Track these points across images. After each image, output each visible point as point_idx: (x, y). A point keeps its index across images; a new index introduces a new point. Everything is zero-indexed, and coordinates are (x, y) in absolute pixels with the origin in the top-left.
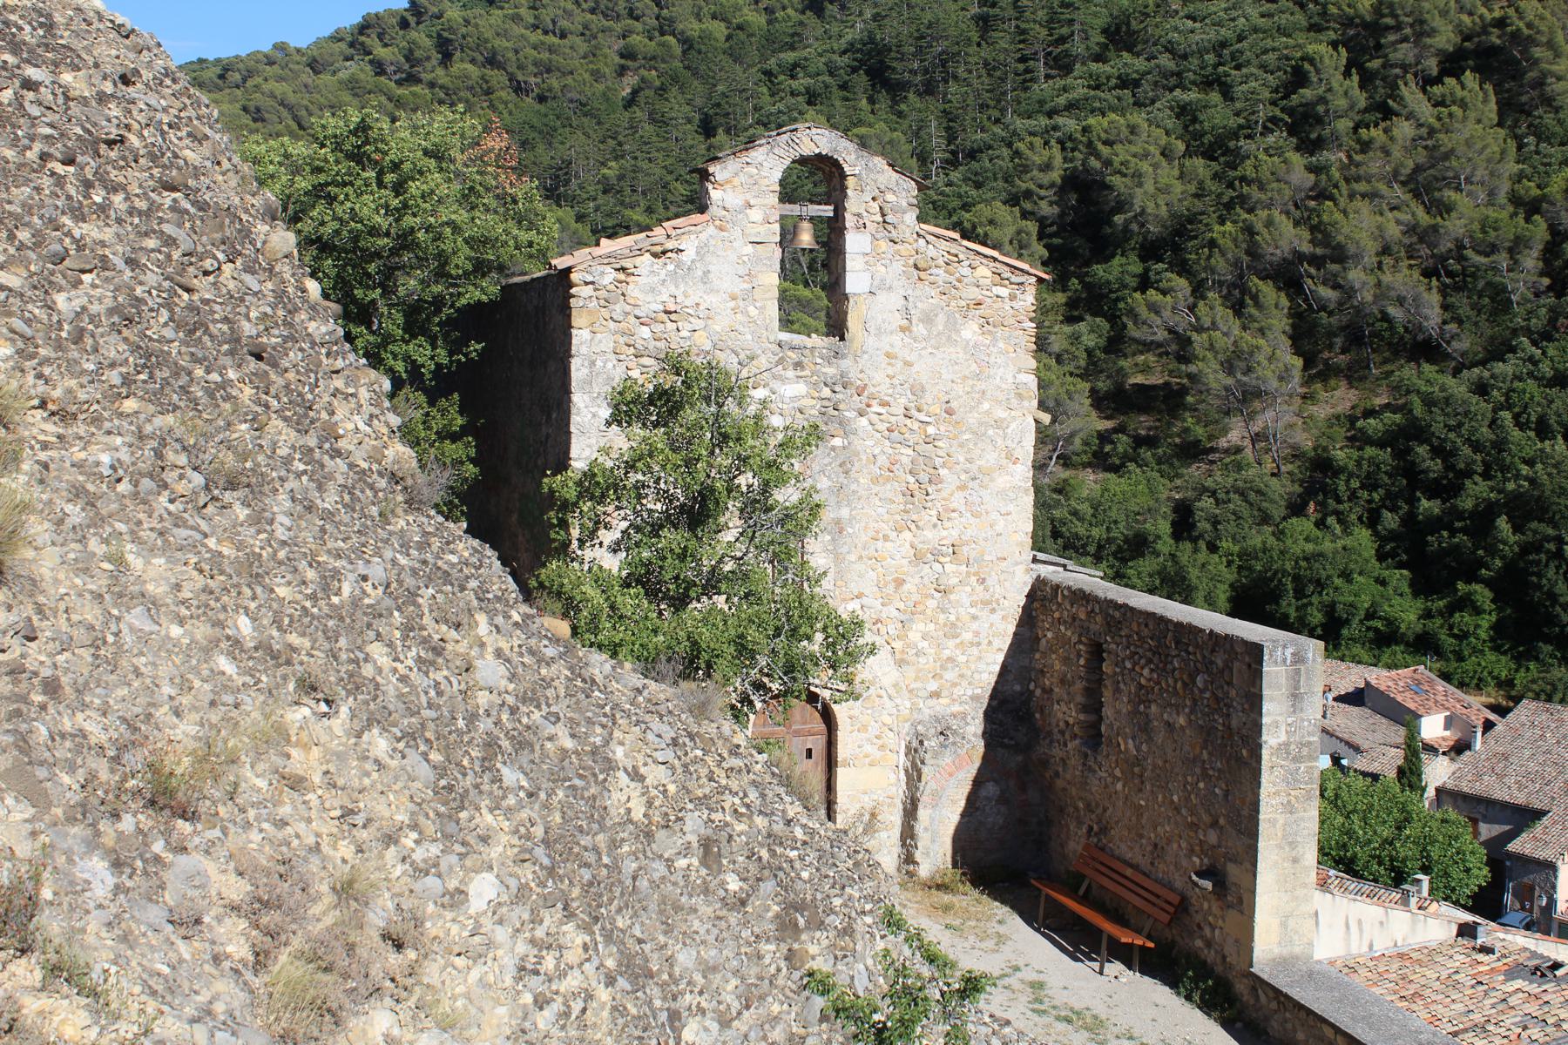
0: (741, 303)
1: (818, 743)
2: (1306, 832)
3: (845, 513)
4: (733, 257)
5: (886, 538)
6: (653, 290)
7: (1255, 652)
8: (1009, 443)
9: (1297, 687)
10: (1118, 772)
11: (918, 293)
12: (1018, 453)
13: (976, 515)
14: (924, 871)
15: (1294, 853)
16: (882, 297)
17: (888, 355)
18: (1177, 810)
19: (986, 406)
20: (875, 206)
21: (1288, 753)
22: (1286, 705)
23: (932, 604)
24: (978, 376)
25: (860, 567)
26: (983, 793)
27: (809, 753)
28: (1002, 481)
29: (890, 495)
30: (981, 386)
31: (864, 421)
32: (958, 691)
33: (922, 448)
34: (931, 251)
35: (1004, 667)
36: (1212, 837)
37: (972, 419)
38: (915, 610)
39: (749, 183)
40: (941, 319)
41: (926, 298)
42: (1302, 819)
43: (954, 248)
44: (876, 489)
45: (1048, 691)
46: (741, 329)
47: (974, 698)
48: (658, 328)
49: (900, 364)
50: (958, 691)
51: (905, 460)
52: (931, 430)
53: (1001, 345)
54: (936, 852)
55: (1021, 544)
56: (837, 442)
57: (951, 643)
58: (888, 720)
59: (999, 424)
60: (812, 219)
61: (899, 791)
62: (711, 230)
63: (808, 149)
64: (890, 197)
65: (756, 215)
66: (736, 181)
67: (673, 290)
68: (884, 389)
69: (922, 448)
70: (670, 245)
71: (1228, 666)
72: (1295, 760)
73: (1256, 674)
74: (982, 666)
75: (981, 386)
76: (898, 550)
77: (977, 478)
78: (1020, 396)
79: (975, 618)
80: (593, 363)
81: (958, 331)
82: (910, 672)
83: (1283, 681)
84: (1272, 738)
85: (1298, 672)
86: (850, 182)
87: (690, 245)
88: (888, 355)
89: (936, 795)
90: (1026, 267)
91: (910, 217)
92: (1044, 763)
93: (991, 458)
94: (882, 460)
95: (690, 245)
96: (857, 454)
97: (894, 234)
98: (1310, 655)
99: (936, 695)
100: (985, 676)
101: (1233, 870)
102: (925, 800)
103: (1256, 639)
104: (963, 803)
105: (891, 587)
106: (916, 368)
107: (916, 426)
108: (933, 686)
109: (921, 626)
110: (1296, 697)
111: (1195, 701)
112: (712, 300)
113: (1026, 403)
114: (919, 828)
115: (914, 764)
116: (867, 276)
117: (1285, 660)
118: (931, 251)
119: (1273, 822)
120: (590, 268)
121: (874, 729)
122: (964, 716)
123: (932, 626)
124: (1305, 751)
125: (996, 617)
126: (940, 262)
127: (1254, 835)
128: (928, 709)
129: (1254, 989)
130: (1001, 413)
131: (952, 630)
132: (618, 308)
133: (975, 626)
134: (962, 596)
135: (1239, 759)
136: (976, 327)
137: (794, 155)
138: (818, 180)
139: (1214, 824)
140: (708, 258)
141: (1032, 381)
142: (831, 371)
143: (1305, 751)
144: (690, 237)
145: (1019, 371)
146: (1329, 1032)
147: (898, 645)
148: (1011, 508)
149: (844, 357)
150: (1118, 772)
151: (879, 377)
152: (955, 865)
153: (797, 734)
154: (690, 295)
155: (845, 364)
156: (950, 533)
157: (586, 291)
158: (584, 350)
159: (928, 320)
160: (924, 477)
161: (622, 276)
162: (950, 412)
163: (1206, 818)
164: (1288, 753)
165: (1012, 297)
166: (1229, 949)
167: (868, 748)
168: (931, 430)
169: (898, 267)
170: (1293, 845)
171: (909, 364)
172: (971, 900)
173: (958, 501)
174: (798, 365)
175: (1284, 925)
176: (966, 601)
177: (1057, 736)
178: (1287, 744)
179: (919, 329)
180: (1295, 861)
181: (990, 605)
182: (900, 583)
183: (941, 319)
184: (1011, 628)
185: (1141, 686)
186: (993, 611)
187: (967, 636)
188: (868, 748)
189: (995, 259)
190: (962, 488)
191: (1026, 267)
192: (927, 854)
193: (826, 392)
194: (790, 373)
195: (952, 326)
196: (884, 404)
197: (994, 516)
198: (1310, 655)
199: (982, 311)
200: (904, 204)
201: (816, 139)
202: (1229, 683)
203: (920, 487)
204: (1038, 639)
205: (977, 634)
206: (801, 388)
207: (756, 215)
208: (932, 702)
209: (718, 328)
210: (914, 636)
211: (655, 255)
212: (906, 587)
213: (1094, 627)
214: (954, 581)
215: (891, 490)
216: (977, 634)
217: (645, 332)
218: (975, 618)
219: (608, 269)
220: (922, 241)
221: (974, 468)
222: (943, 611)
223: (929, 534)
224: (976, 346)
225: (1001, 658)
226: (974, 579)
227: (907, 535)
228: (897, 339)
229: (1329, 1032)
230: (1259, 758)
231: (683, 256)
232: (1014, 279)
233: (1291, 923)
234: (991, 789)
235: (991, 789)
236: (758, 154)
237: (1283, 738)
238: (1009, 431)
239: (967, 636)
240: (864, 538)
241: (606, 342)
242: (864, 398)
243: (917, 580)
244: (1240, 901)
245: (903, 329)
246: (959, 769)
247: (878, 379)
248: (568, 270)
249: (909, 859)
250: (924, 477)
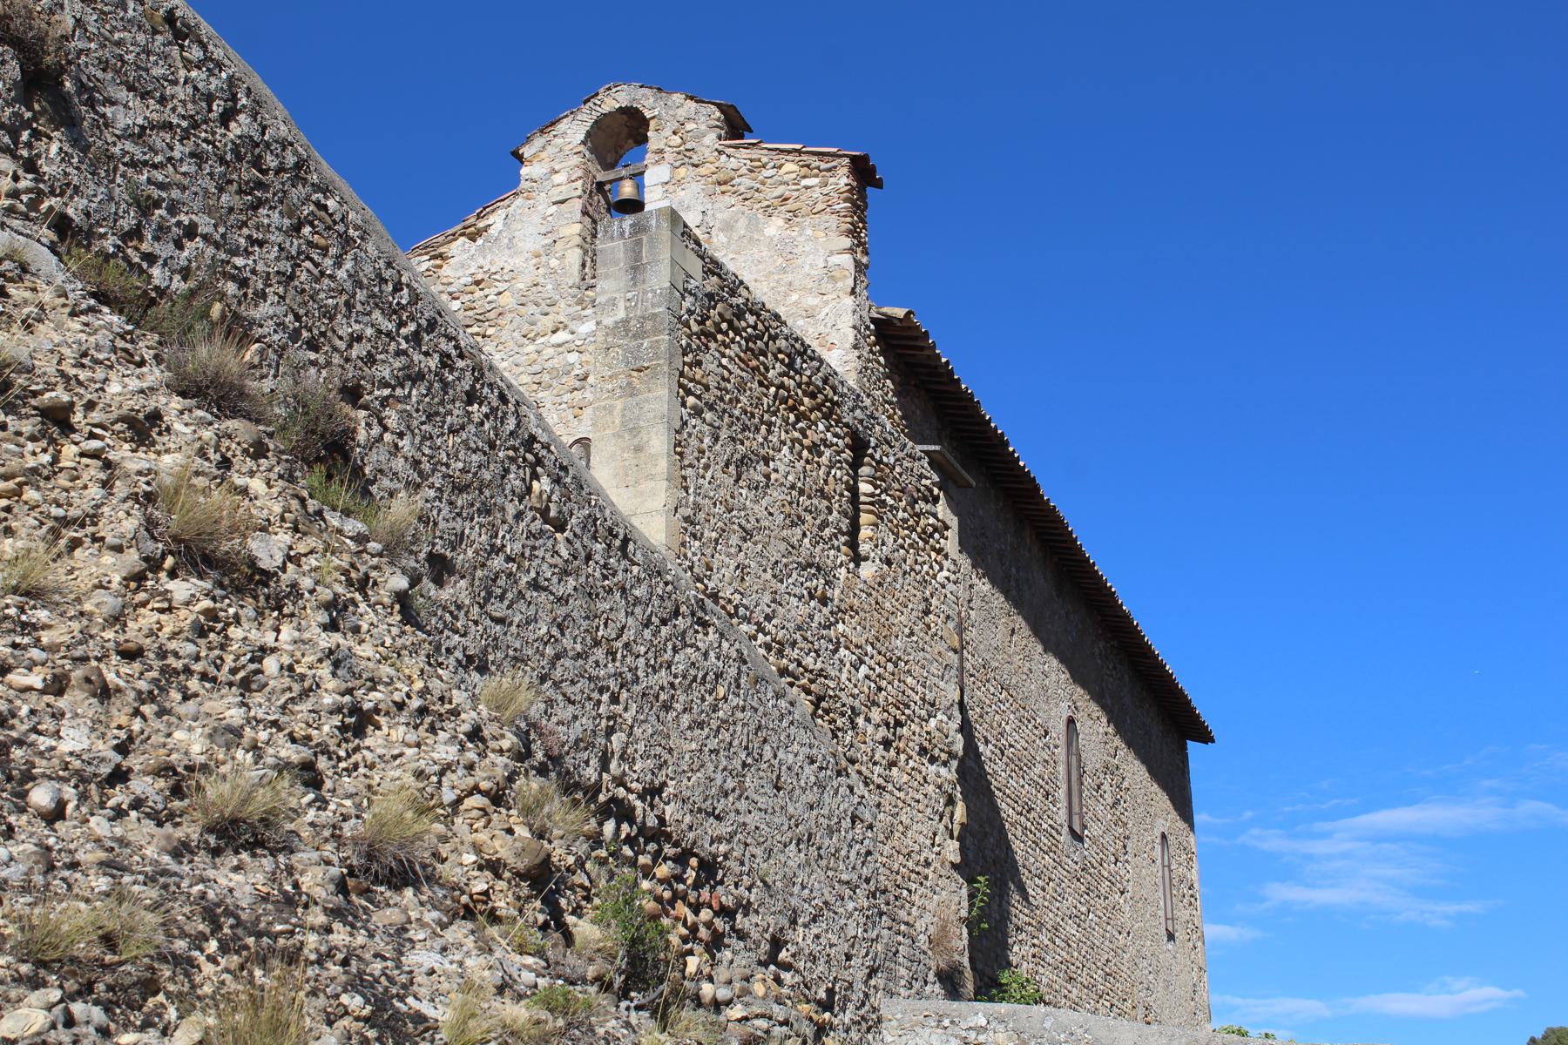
0: (544, 259)
2: (651, 415)
4: (536, 219)
8: (821, 329)
11: (717, 206)
15: (636, 442)
20: (676, 140)
21: (627, 331)
22: (624, 279)
30: (790, 277)
34: (733, 163)
42: (647, 400)
43: (755, 153)
46: (541, 280)
53: (809, 232)
62: (519, 201)
64: (690, 126)
65: (560, 178)
66: (543, 155)
67: (481, 261)
70: (481, 224)
72: (635, 337)
75: (790, 277)
78: (833, 279)
81: (760, 231)
85: (639, 243)
87: (496, 220)
91: (711, 139)
97: (695, 160)
98: (653, 222)
110: (636, 268)
112: (517, 262)
113: (840, 285)
117: (622, 234)
118: (733, 163)
124: (649, 325)
126: (744, 170)
130: (812, 301)
136: (781, 222)
137: (595, 115)
140: (515, 226)
141: (847, 260)
145: (831, 253)
161: (438, 262)
164: (627, 331)
169: (695, 187)
170: (634, 431)
178: (626, 321)
183: (743, 222)
189: (799, 152)
195: (753, 225)
198: (653, 222)
199: (791, 205)
200: (703, 127)
209: (521, 286)
211: (473, 238)
220: (723, 157)
224: (782, 240)
231: (491, 231)
232: (823, 166)
237: (621, 314)
238: (821, 316)
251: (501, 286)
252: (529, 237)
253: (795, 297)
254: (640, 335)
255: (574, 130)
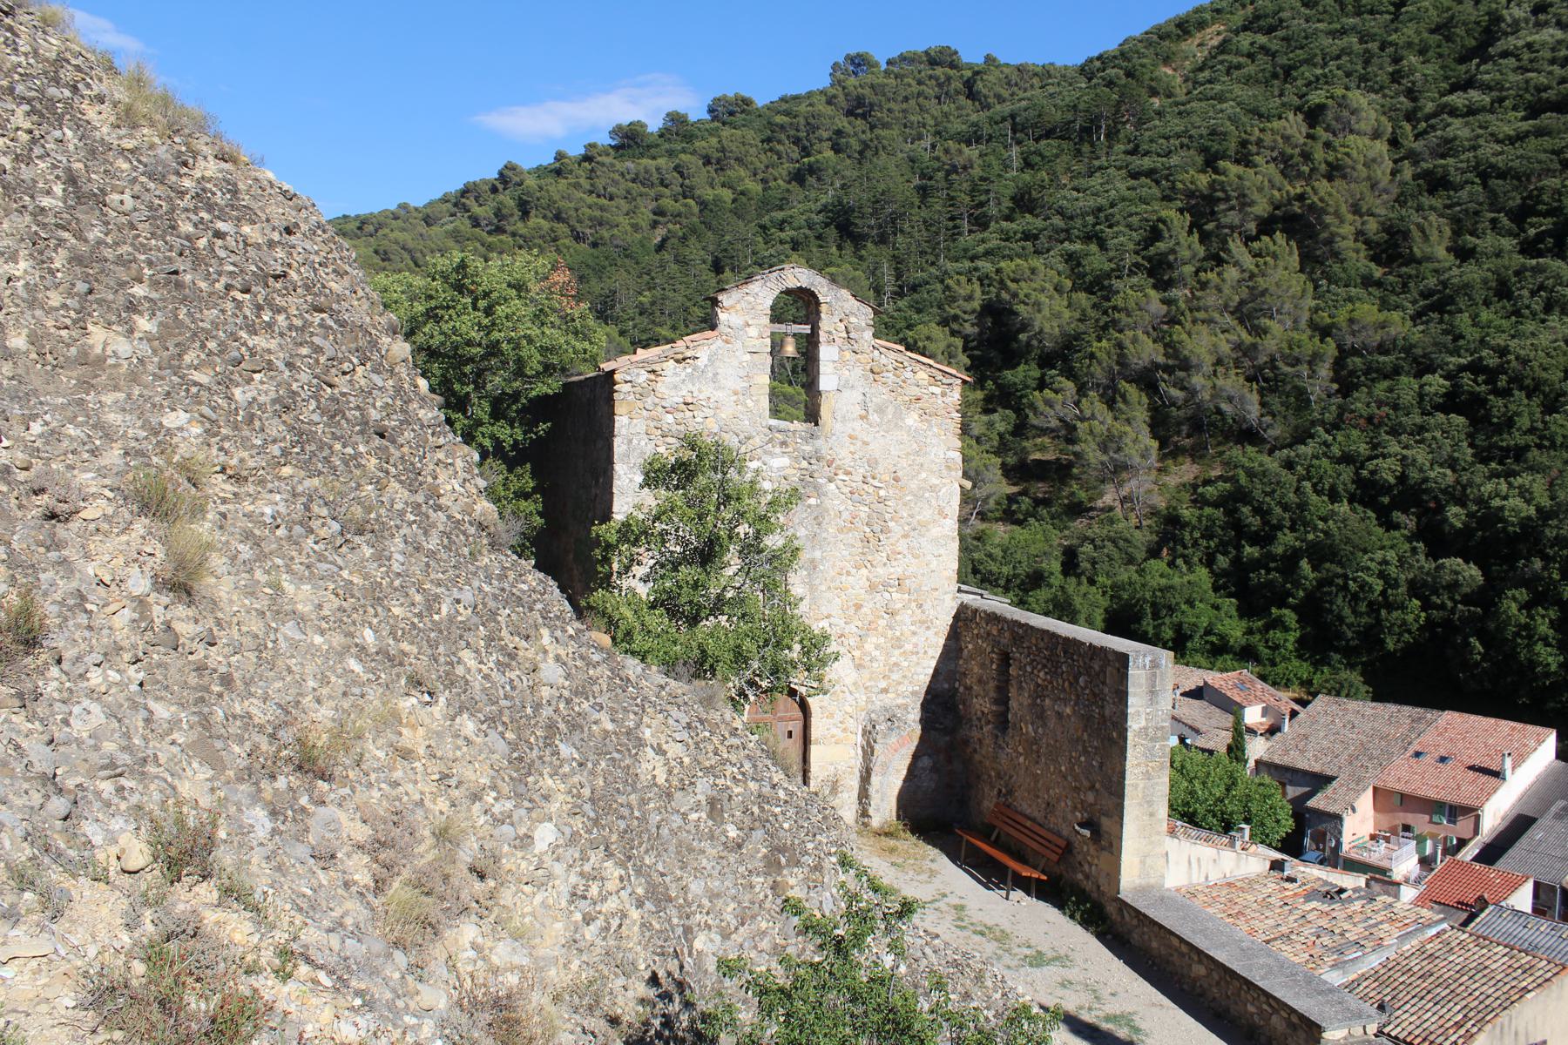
1: (796, 727)
3: (818, 554)
5: (848, 573)
6: (675, 387)
7: (1123, 659)
9: (1153, 686)
10: (1020, 749)
12: (948, 510)
13: (916, 557)
14: (876, 822)
16: (846, 393)
17: (851, 437)
18: (1065, 777)
19: (924, 475)
20: (842, 326)
23: (882, 623)
24: (917, 453)
25: (828, 595)
26: (920, 764)
27: (790, 734)
28: (935, 531)
29: (852, 541)
30: (920, 460)
31: (832, 486)
32: (902, 688)
33: (876, 506)
34: (883, 360)
35: (936, 670)
36: (1090, 797)
37: (914, 485)
38: (870, 627)
39: (747, 309)
40: (891, 410)
41: (880, 395)
43: (900, 358)
44: (841, 537)
45: (968, 688)
47: (914, 693)
48: (679, 415)
49: (859, 443)
50: (902, 688)
51: (863, 515)
52: (882, 493)
54: (885, 807)
55: (949, 578)
56: (812, 501)
57: (897, 652)
58: (849, 710)
59: (933, 488)
60: (794, 335)
61: (857, 762)
62: (719, 343)
63: (792, 283)
64: (853, 319)
65: (753, 332)
66: (738, 307)
68: (847, 462)
69: (876, 506)
70: (688, 354)
71: (1103, 670)
73: (1123, 676)
74: (920, 670)
75: (920, 460)
76: (857, 582)
77: (917, 528)
78: (948, 468)
79: (914, 633)
80: (630, 441)
82: (866, 674)
83: (1143, 681)
84: (1135, 724)
85: (1154, 675)
86: (823, 308)
88: (851, 437)
89: (885, 766)
90: (953, 372)
91: (868, 334)
92: (966, 742)
93: (927, 514)
94: (846, 515)
95: (703, 355)
96: (827, 511)
97: (856, 347)
99: (885, 691)
100: (922, 677)
101: (1105, 822)
102: (876, 769)
103: (1123, 650)
104: (905, 772)
105: (852, 611)
106: (871, 447)
107: (871, 490)
108: (883, 684)
109: (874, 640)
110: (1153, 693)
111: (1078, 696)
112: (720, 395)
114: (872, 791)
115: (868, 743)
116: (835, 378)
118: (883, 360)
119: (1136, 786)
120: (630, 371)
121: (838, 716)
122: (905, 707)
123: (882, 640)
124: (1159, 734)
125: (930, 633)
126: (890, 367)
127: (1121, 796)
128: (879, 701)
129: (1120, 910)
130: (935, 481)
131: (897, 643)
132: (650, 400)
133: (914, 639)
134: (905, 617)
135: (1111, 739)
136: (916, 417)
138: (800, 306)
139: (1092, 787)
140: (717, 363)
141: (958, 457)
142: (808, 448)
143: (1159, 734)
144: (703, 347)
146: (1175, 942)
147: (857, 653)
148: (942, 551)
149: (818, 438)
150: (1020, 749)
151: (844, 453)
152: (898, 818)
153: (781, 719)
154: (703, 391)
155: (819, 443)
156: (896, 570)
157: (626, 388)
158: (624, 431)
159: (880, 410)
160: (877, 528)
161: (652, 377)
162: (896, 480)
163: (1086, 783)
165: (944, 395)
166: (1102, 881)
167: (834, 731)
168: (882, 493)
169: (858, 371)
170: (1150, 803)
171: (866, 443)
172: (911, 845)
173: (902, 546)
174: (784, 444)
175: (1143, 862)
176: (908, 621)
177: (975, 722)
178: (1146, 728)
179: (874, 417)
180: (1152, 815)
181: (926, 624)
182: (858, 607)
183: (891, 410)
184: (942, 641)
185: (1038, 685)
186: (928, 628)
187: (908, 647)
188: (834, 731)
190: (905, 536)
191: (953, 372)
192: (878, 810)
193: (804, 464)
194: (778, 450)
195: (898, 415)
196: (848, 473)
197: (929, 557)
201: (798, 276)
202: (1104, 683)
203: (874, 536)
204: (961, 650)
205: (916, 645)
206: (786, 461)
207: (753, 332)
208: (882, 696)
210: (869, 647)
211: (677, 361)
212: (864, 610)
213: (1004, 641)
214: (899, 606)
215: (852, 537)
216: (916, 645)
217: (669, 418)
218: (914, 633)
219: (643, 372)
221: (915, 522)
222: (891, 628)
223: (880, 570)
225: (933, 663)
226: (914, 605)
227: (864, 571)
228: (858, 425)
229: (1175, 942)
230: (1125, 739)
231: (698, 362)
233: (1149, 861)
234: (926, 762)
235: (926, 762)
236: (755, 287)
237: (1143, 723)
239: (908, 647)
240: (832, 573)
241: (640, 425)
242: (832, 469)
243: (871, 605)
244: (1111, 845)
245: (862, 418)
246: (902, 745)
247: (843, 454)
248: (613, 372)
249: (864, 814)
250: (877, 528)
251: (709, 412)
252: (731, 379)
253: (924, 475)
254: (1153, 739)
255: (761, 294)
